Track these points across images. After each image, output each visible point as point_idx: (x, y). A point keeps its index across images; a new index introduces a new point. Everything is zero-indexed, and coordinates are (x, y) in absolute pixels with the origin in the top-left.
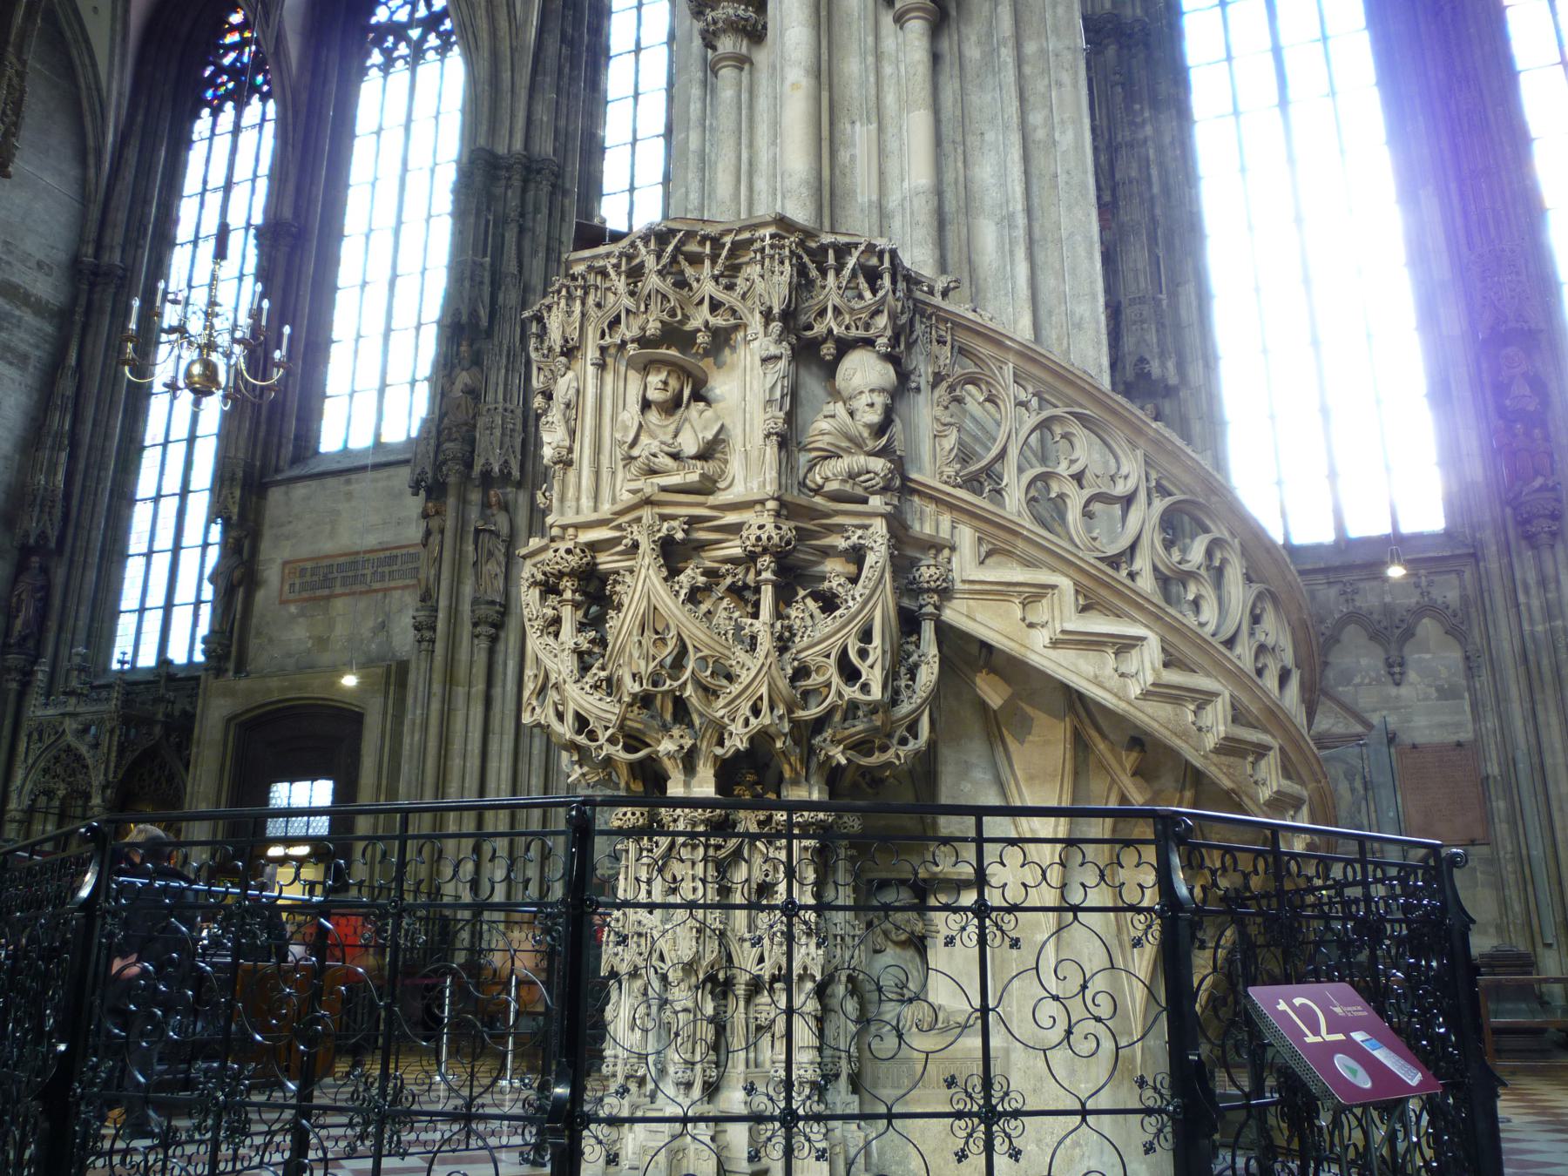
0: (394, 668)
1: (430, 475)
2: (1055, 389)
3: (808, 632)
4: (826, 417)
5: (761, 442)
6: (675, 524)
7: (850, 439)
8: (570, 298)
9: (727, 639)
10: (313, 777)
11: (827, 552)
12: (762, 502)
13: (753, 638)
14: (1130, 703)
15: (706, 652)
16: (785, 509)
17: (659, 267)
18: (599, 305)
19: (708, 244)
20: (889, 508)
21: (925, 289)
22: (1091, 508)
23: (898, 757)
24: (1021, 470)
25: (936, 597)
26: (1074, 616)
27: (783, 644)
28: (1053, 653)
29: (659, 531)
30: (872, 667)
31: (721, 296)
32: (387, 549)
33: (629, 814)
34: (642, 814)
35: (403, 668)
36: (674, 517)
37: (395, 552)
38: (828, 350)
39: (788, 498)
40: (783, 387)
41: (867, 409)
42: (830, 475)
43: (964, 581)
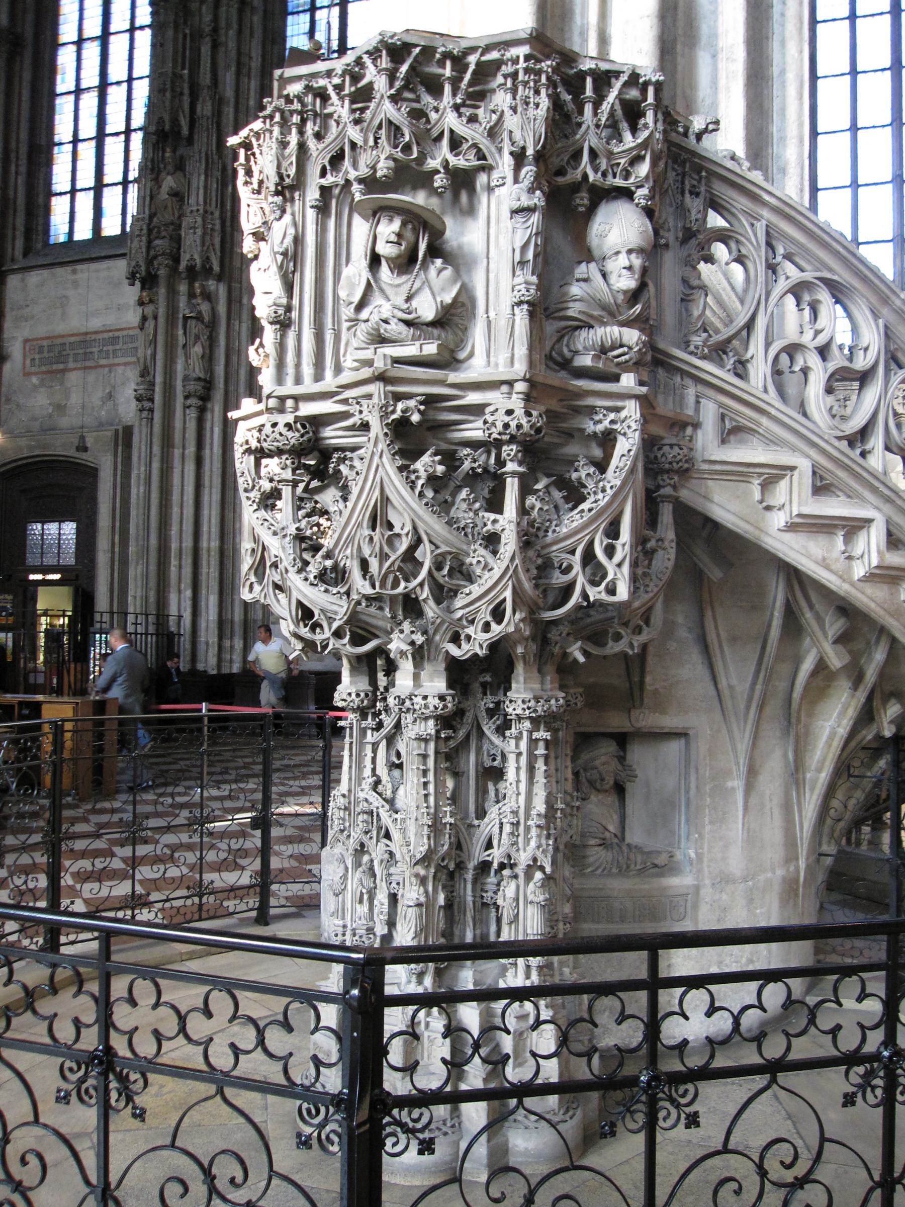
1: (143, 268)
2: (807, 250)
4: (578, 280)
5: (509, 311)
7: (604, 307)
8: (284, 124)
9: (466, 535)
12: (510, 383)
14: (852, 584)
15: (444, 549)
17: (393, 91)
18: (319, 136)
19: (448, 64)
20: (644, 390)
21: (681, 130)
23: (631, 646)
25: (676, 478)
26: (811, 500)
28: (788, 537)
29: (393, 412)
30: (619, 565)
31: (461, 129)
32: (110, 331)
33: (353, 696)
34: (367, 695)
35: (128, 431)
36: (409, 396)
37: (117, 334)
38: (583, 200)
40: (536, 245)
41: (625, 272)
43: (704, 461)
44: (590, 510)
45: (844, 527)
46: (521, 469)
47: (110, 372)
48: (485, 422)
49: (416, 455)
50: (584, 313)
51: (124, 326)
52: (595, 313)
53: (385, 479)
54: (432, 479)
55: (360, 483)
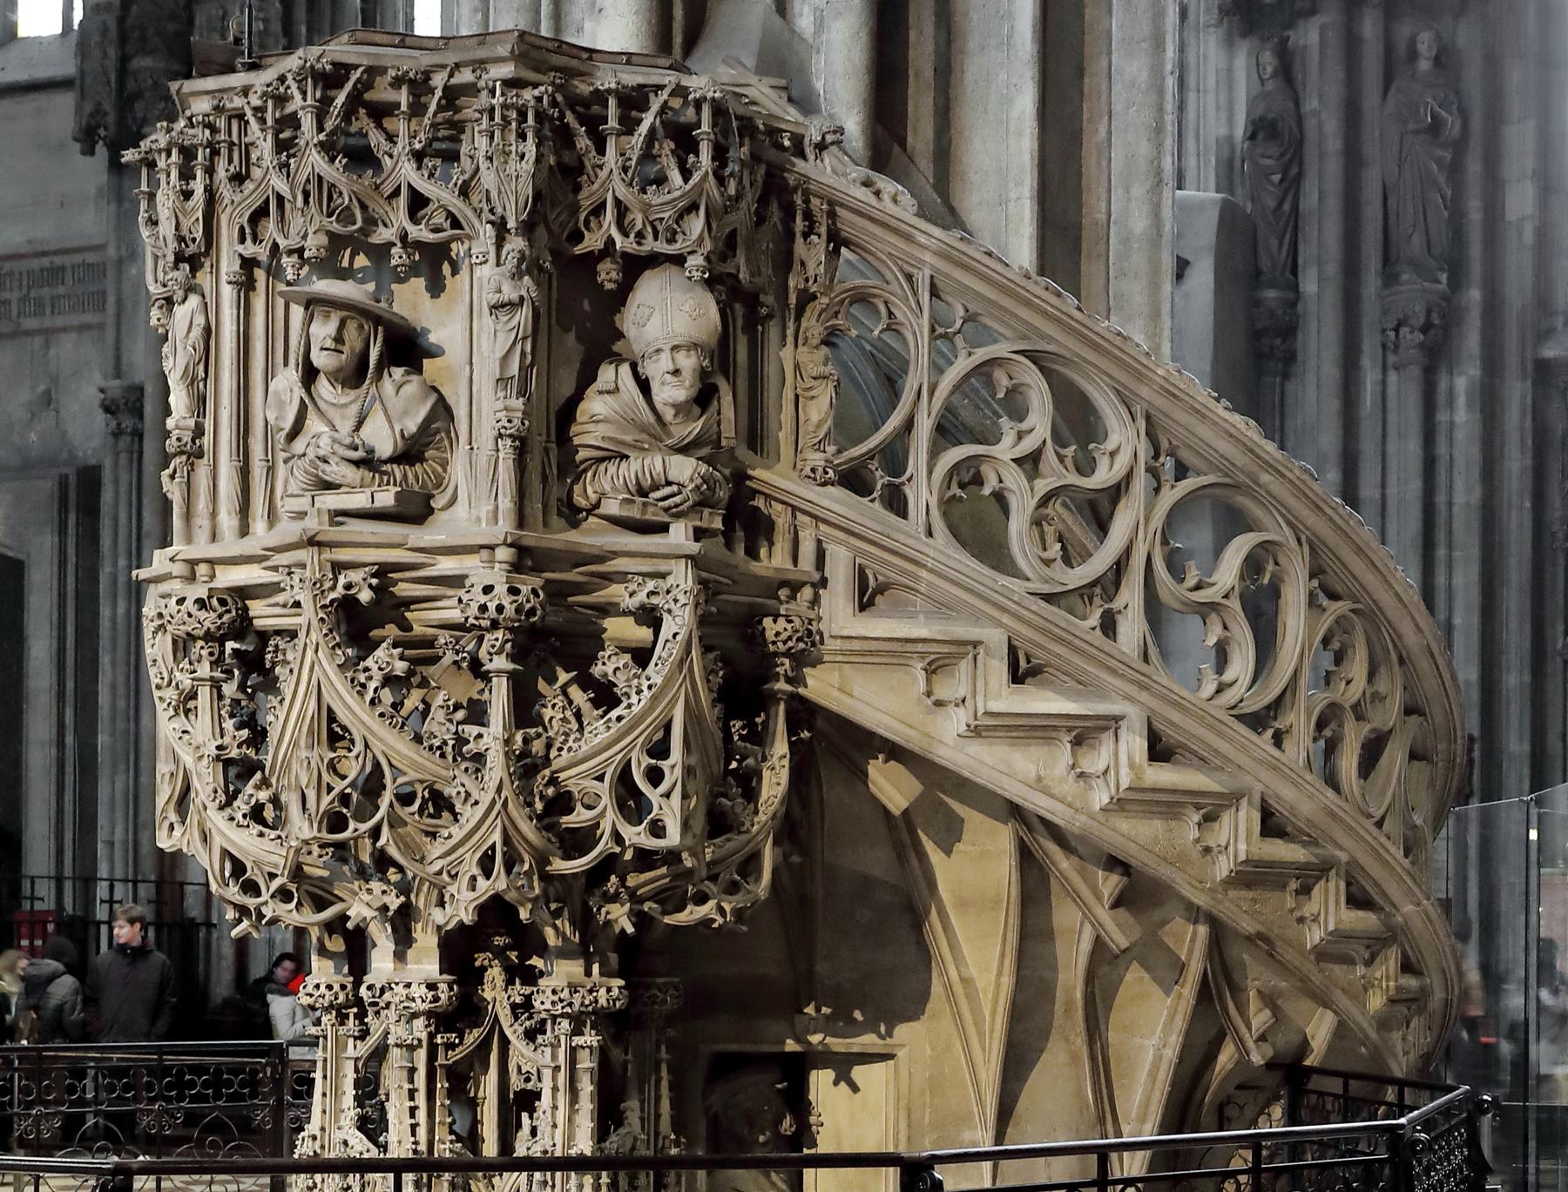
0: (73, 479)
1: (111, 119)
3: (570, 743)
4: (601, 393)
5: (491, 445)
6: (355, 576)
9: (443, 756)
11: (607, 610)
12: (492, 548)
13: (479, 758)
15: (413, 775)
16: (525, 559)
22: (1049, 511)
24: (934, 455)
27: (526, 767)
29: (333, 588)
30: (667, 795)
32: (44, 254)
35: (90, 479)
37: (58, 260)
38: (608, 274)
39: (530, 538)
40: (523, 354)
42: (608, 488)
44: (619, 719)
45: (1070, 730)
46: (511, 666)
47: (47, 345)
48: (460, 601)
49: (367, 646)
50: (610, 439)
51: (76, 243)
52: (628, 438)
53: (323, 681)
54: (389, 680)
55: (292, 687)
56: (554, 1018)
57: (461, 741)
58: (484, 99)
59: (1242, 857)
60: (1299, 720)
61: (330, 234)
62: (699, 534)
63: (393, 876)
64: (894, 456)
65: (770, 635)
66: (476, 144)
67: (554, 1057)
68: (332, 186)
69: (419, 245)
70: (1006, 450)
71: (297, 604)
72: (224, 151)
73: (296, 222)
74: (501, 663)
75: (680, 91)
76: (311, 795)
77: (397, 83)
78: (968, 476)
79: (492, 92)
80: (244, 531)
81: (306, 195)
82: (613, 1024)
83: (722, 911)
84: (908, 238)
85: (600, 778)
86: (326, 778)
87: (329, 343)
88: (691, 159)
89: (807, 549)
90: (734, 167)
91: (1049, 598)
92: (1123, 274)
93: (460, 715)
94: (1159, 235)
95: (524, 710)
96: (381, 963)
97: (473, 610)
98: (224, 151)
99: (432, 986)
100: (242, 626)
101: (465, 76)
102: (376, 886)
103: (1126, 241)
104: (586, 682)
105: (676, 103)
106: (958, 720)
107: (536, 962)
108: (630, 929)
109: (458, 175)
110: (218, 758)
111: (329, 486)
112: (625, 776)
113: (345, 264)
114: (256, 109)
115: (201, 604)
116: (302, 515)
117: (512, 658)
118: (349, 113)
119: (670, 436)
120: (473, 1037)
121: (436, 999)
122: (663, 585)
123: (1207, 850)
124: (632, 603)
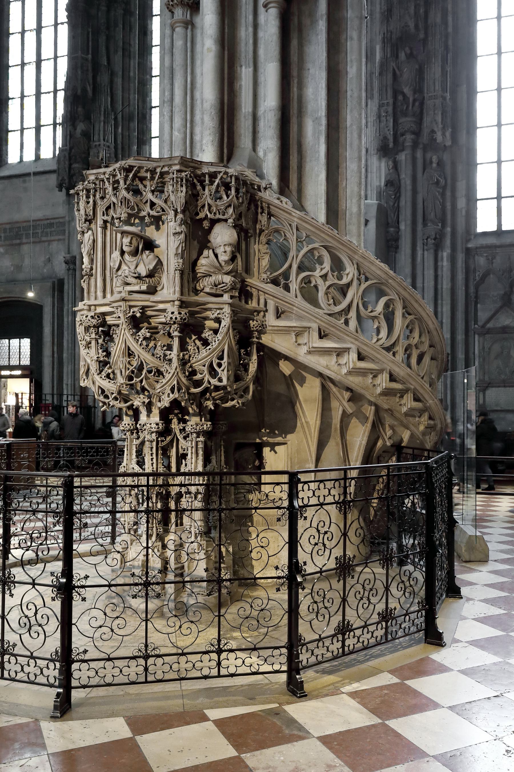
0: (56, 282)
1: (67, 181)
5: (173, 272)
6: (135, 309)
10: (20, 336)
11: (206, 318)
12: (174, 301)
13: (170, 360)
15: (152, 365)
16: (183, 304)
22: (330, 290)
24: (297, 275)
27: (184, 363)
30: (223, 370)
32: (48, 219)
35: (61, 283)
37: (52, 221)
38: (206, 224)
39: (184, 298)
40: (182, 247)
44: (210, 349)
45: (336, 352)
46: (179, 334)
47: (49, 245)
49: (139, 329)
51: (57, 216)
52: (212, 270)
54: (145, 338)
56: (192, 433)
57: (165, 355)
58: (171, 175)
59: (384, 387)
60: (400, 349)
61: (128, 214)
62: (232, 297)
63: (146, 393)
64: (286, 275)
65: (252, 325)
66: (169, 188)
67: (192, 444)
68: (129, 200)
69: (153, 216)
70: (317, 273)
71: (119, 317)
72: (98, 190)
73: (119, 210)
74: (176, 333)
75: (226, 173)
76: (123, 371)
77: (147, 171)
78: (307, 281)
79: (173, 173)
80: (104, 297)
81: (121, 202)
82: (208, 435)
83: (238, 403)
84: (290, 214)
85: (204, 366)
86: (127, 366)
87: (128, 244)
88: (229, 192)
89: (262, 301)
90: (241, 194)
91: (329, 315)
92: (350, 224)
93: (165, 348)
94: (360, 213)
95: (183, 347)
96: (143, 418)
97: (169, 319)
98: (98, 190)
99: (157, 424)
100: (104, 323)
101: (166, 169)
102: (142, 396)
103: (351, 215)
104: (200, 339)
105: (225, 176)
106: (304, 349)
107: (187, 417)
108: (213, 408)
109: (164, 197)
110: (97, 361)
111: (128, 284)
112: (211, 365)
113: (132, 222)
114: (107, 179)
115: (92, 317)
116: (120, 292)
117: (179, 332)
118: (133, 179)
119: (223, 269)
120: (169, 438)
121: (158, 428)
122: (222, 312)
123: (374, 385)
124: (213, 317)
